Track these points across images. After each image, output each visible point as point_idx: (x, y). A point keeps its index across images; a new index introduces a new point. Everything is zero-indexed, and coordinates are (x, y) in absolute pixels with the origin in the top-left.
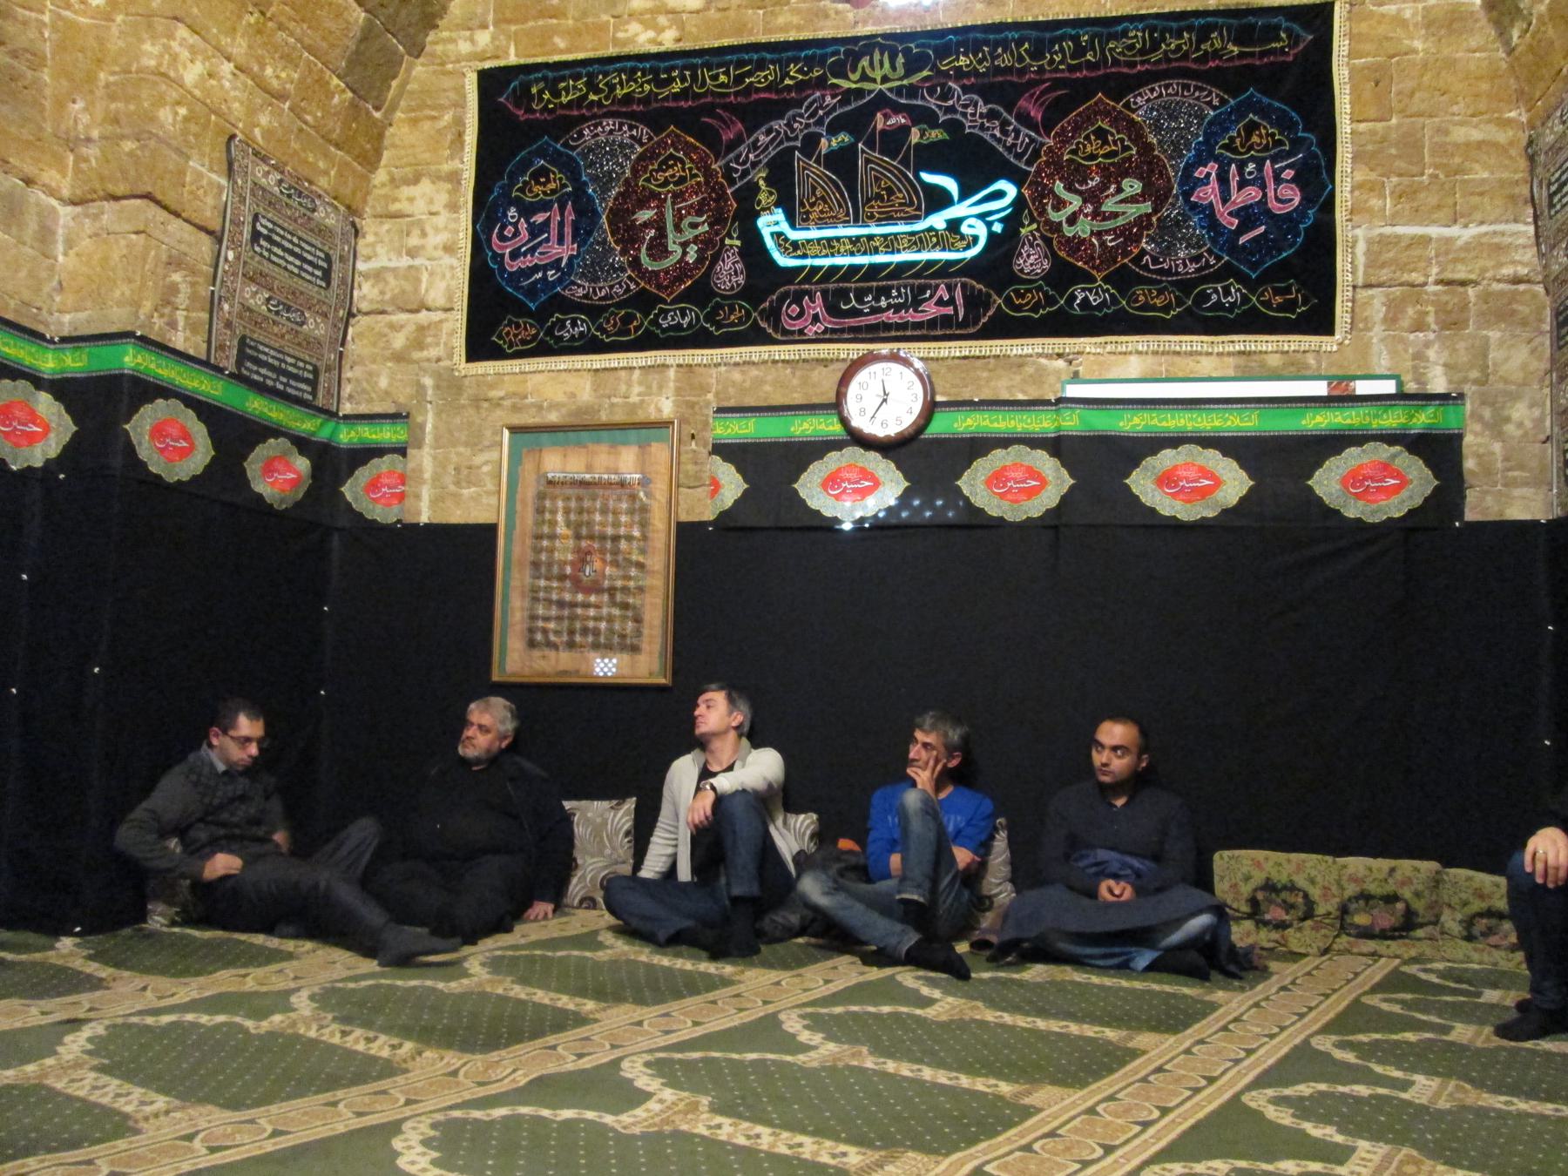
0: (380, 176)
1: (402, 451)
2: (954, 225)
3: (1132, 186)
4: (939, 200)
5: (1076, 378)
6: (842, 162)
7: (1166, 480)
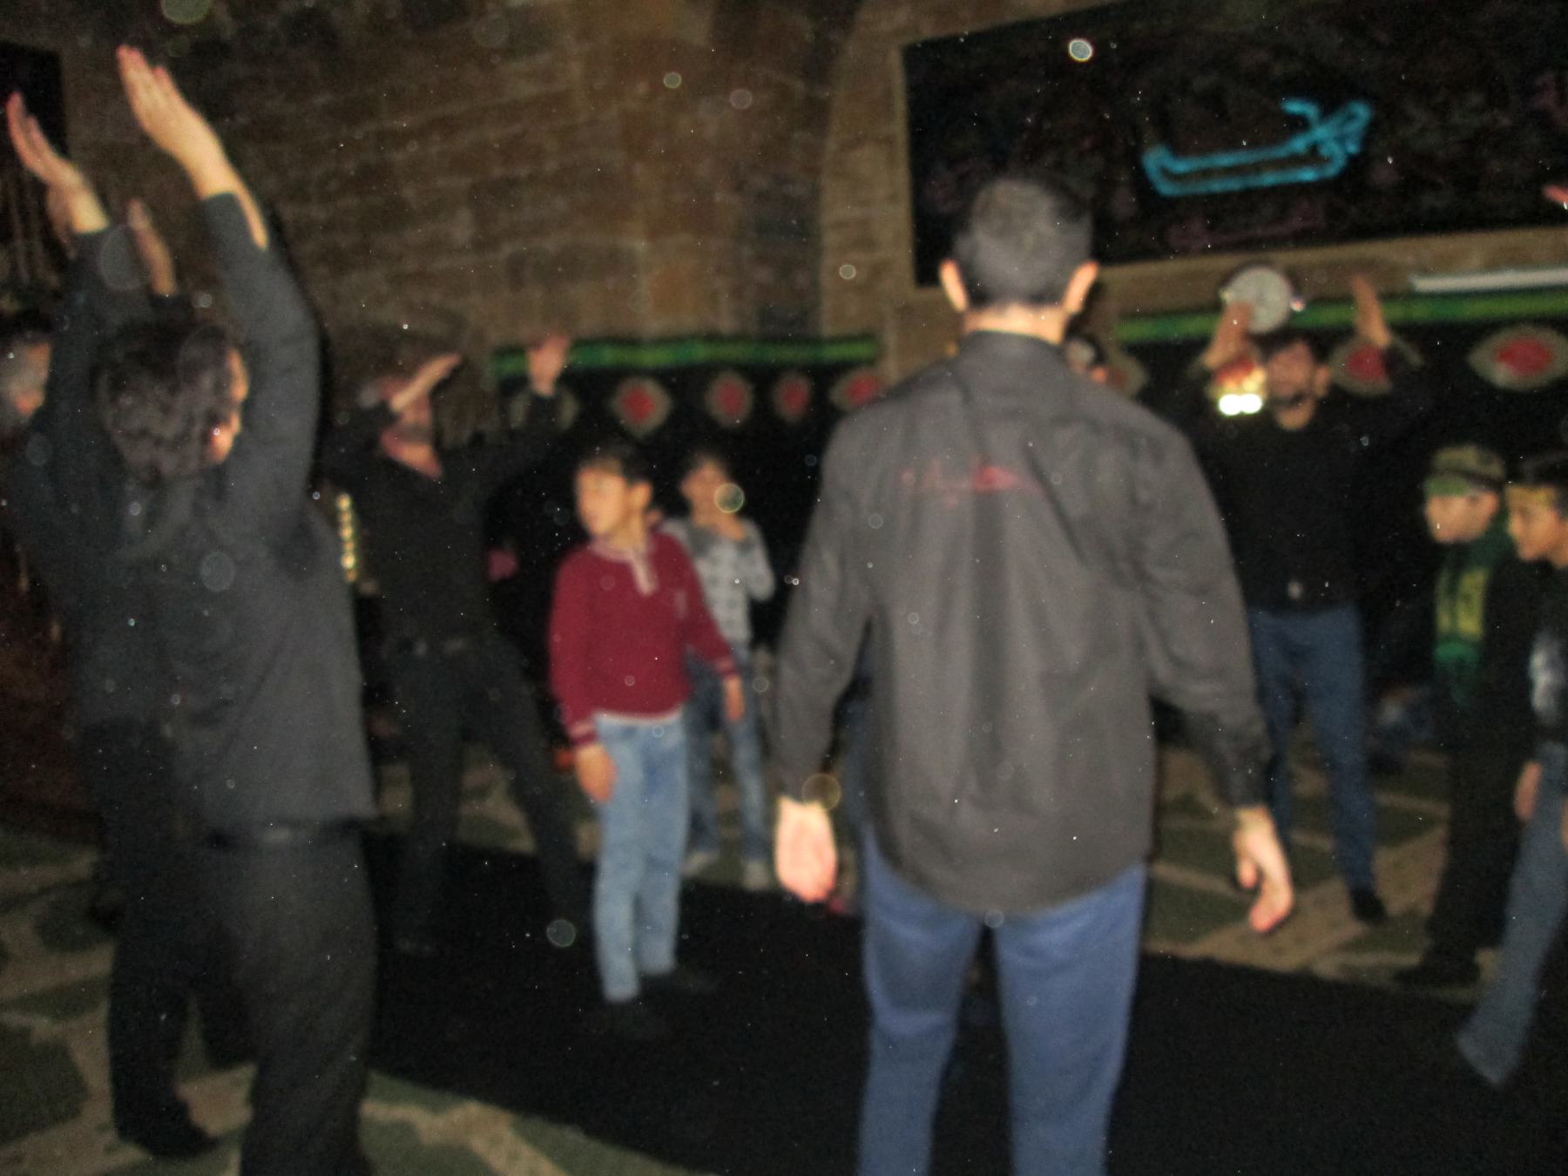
0: (831, 145)
1: (871, 362)
2: (1314, 149)
3: (1476, 99)
4: (1299, 124)
5: (1425, 272)
6: (1214, 100)
7: (1506, 355)
